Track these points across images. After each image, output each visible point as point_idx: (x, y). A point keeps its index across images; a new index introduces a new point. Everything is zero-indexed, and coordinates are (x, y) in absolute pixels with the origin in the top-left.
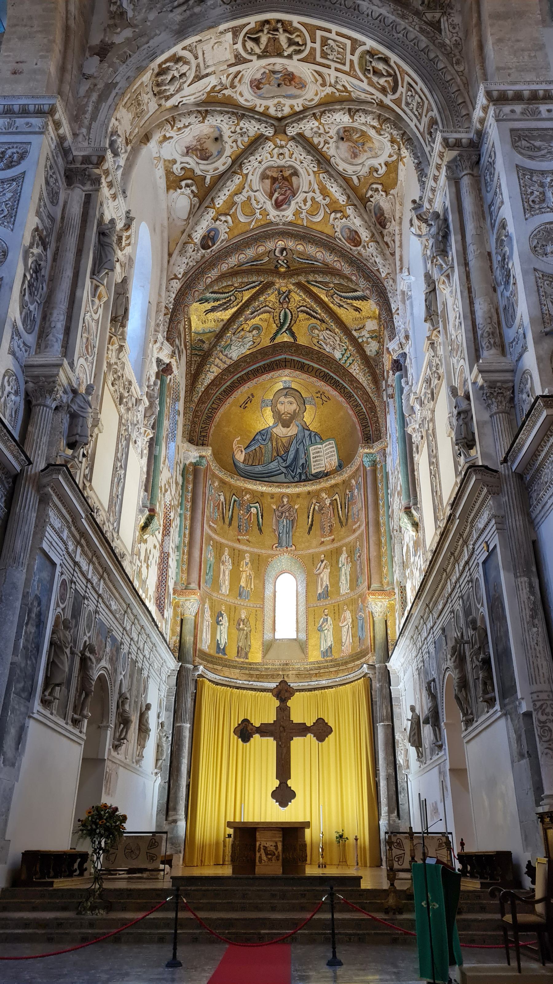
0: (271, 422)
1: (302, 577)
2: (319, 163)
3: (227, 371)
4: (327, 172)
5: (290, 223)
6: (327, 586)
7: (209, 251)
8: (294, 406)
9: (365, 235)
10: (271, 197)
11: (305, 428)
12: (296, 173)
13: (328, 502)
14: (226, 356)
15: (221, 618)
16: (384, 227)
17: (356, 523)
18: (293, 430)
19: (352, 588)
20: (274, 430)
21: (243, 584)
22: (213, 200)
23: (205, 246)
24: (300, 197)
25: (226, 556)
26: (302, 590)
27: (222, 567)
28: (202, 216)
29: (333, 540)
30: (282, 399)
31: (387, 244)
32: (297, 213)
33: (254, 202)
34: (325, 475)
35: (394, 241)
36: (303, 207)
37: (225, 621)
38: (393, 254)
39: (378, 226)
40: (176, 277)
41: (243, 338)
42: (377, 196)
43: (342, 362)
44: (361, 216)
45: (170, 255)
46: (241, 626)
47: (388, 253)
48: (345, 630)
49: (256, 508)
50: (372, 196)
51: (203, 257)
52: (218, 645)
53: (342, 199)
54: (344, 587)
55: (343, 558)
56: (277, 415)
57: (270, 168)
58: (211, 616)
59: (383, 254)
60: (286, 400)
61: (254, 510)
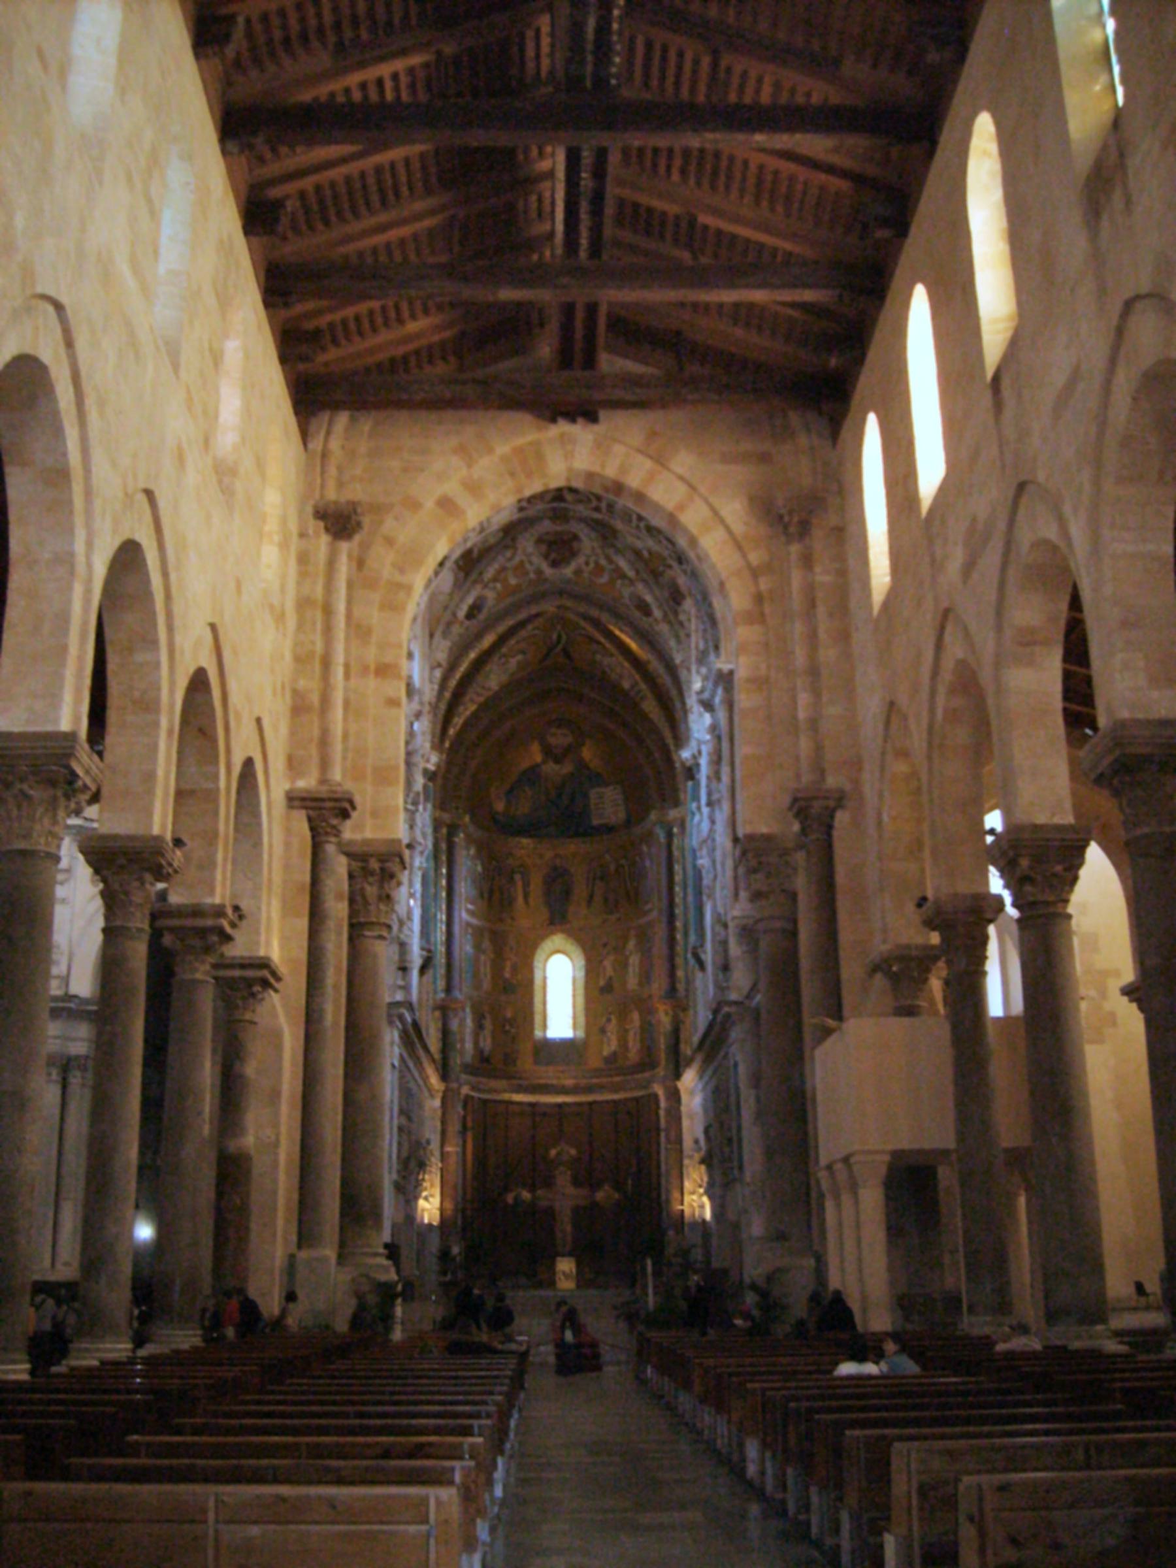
0: (539, 758)
1: (581, 962)
2: (604, 538)
3: (484, 707)
4: (613, 546)
5: (569, 581)
6: (610, 978)
7: (474, 621)
8: (570, 739)
9: (657, 613)
10: (546, 557)
11: (582, 765)
12: (576, 537)
13: (612, 867)
14: (483, 687)
15: (483, 1022)
16: (679, 603)
17: (647, 903)
18: (567, 768)
19: (640, 984)
20: (544, 767)
21: (507, 975)
22: (481, 574)
23: (470, 616)
24: (581, 560)
25: (486, 944)
26: (581, 974)
27: (483, 958)
28: (468, 592)
29: (619, 919)
30: (553, 730)
31: (681, 624)
32: (578, 572)
33: (528, 566)
34: (610, 829)
35: (689, 620)
36: (584, 567)
37: (488, 1024)
38: (688, 636)
39: (671, 603)
40: (439, 665)
41: (504, 664)
42: (669, 573)
43: (632, 694)
44: (651, 591)
45: (432, 635)
46: (507, 1028)
47: (682, 634)
48: (631, 1034)
49: (522, 873)
50: (664, 571)
51: (467, 628)
52: (482, 1052)
53: (631, 574)
54: (632, 982)
55: (631, 944)
56: (548, 752)
57: (547, 533)
58: (473, 1020)
59: (677, 637)
60: (559, 731)
61: (517, 877)
